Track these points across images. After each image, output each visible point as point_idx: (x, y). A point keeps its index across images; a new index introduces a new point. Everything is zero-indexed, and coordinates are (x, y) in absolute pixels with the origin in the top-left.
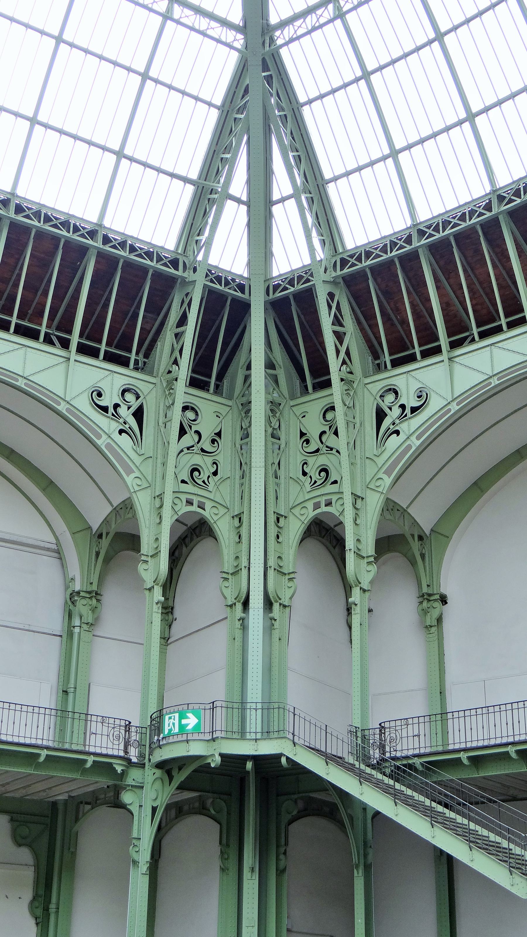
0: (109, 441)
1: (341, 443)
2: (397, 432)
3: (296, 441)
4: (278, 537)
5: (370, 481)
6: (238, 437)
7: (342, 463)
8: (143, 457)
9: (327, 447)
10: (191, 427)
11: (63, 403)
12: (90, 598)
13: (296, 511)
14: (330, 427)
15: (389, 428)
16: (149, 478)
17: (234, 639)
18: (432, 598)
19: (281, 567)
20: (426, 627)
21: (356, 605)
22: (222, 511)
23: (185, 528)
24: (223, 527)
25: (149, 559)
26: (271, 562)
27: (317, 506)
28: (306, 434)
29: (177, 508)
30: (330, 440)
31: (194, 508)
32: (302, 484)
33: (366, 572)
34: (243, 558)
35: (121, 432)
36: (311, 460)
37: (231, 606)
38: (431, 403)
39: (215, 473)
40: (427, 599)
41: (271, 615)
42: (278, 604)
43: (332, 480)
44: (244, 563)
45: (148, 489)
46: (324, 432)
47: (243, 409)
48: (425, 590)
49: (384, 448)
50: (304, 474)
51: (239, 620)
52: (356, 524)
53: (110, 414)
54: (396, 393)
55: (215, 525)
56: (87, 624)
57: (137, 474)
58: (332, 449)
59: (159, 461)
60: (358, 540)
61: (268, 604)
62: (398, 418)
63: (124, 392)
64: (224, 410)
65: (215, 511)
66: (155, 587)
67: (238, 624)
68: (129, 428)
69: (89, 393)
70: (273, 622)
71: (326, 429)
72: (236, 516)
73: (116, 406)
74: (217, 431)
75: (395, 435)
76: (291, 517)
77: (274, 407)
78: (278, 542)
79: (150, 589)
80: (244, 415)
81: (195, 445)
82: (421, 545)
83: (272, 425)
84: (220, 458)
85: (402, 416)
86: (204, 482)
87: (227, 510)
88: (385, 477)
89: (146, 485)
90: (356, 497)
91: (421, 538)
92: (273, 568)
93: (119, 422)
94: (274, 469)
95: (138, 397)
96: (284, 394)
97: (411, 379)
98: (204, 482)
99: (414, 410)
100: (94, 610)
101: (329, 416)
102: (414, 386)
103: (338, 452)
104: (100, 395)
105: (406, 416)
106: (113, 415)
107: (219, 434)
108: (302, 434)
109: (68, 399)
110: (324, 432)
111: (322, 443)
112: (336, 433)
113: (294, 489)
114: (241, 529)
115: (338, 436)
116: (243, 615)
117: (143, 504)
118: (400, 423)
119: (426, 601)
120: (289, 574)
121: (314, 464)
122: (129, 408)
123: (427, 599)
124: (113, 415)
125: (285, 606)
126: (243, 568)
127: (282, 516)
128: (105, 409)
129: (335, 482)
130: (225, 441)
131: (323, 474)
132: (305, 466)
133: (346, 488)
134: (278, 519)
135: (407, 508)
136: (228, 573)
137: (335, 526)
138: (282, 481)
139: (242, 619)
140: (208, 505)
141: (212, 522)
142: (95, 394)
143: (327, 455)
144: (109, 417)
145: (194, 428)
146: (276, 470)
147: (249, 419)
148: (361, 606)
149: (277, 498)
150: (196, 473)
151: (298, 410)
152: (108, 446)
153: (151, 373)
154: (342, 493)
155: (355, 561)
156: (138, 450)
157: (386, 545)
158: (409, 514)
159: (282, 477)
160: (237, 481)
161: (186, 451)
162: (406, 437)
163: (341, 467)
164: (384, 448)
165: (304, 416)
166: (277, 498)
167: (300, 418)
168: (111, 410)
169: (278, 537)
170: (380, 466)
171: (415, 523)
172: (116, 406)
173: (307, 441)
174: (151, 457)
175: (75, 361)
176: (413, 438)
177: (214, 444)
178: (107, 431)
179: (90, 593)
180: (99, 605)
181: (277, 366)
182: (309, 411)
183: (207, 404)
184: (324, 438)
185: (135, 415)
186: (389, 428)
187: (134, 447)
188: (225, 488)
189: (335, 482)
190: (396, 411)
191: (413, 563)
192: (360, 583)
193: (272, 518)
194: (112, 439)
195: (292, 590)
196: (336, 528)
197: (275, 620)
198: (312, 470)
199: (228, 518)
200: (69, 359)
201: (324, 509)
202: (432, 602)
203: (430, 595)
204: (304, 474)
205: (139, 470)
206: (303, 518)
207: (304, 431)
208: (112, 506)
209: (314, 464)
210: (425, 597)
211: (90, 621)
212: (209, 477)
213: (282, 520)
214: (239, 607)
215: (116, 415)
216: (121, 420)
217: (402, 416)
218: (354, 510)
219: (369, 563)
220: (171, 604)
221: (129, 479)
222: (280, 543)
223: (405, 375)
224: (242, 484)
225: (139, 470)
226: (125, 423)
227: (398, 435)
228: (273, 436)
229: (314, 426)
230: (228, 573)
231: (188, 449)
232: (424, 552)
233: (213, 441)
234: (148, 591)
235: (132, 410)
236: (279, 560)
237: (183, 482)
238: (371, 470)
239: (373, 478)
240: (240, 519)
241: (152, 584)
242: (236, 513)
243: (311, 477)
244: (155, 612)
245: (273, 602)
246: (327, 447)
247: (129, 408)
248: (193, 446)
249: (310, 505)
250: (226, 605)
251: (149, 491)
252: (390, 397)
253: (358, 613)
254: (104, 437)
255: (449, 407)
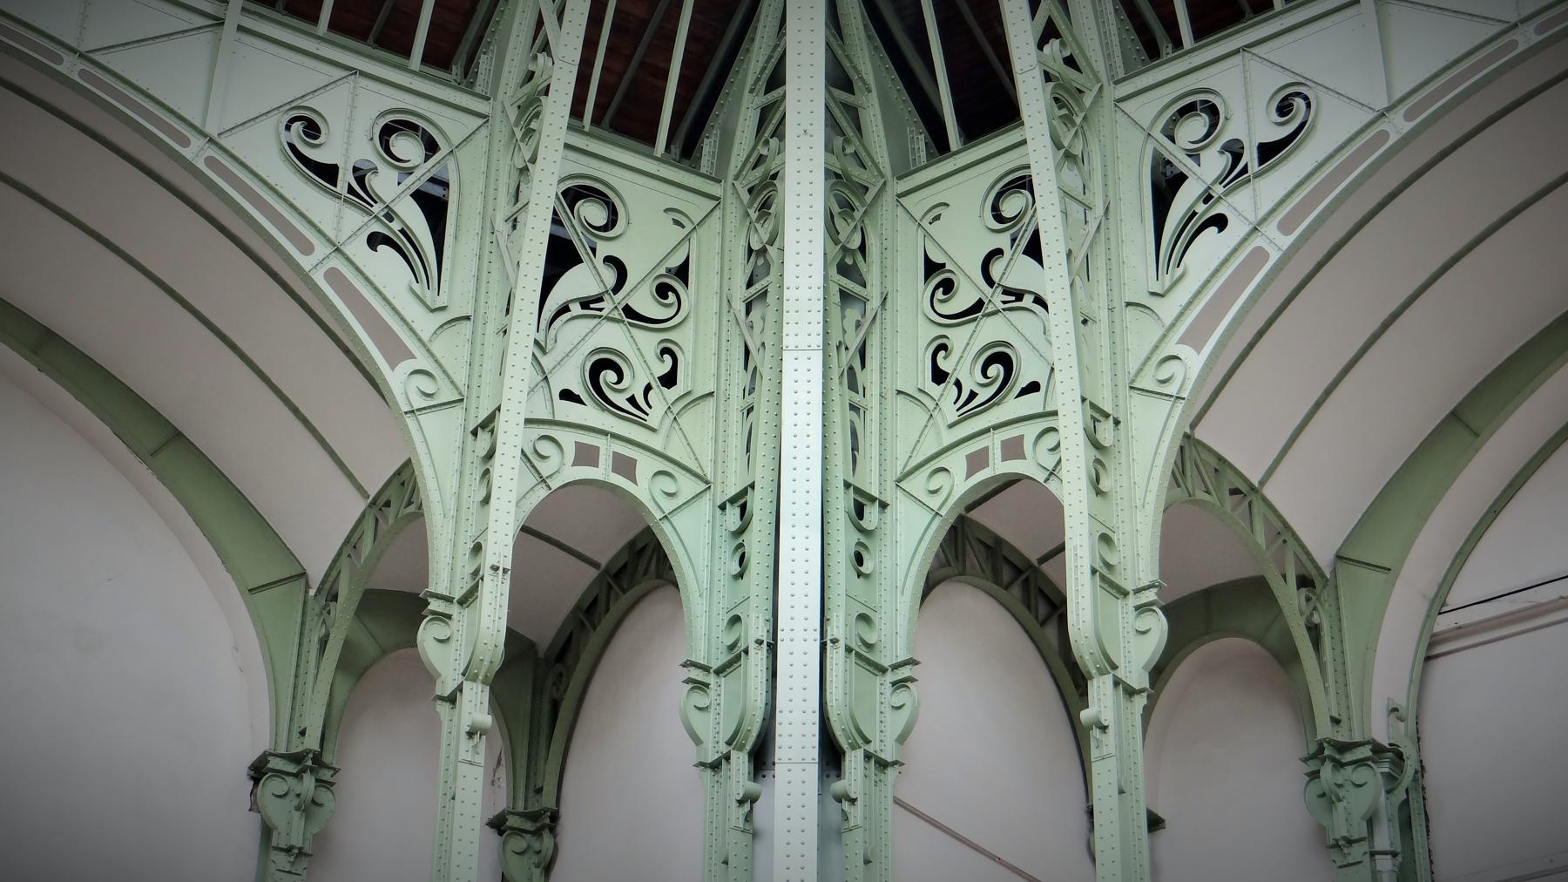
0: (337, 263)
1: (1051, 277)
2: (1220, 222)
3: (912, 290)
4: (859, 559)
5: (1140, 370)
6: (740, 278)
7: (1054, 332)
8: (442, 317)
9: (1007, 291)
10: (594, 250)
11: (197, 142)
12: (298, 776)
13: (917, 484)
14: (1013, 240)
15: (1195, 213)
16: (461, 378)
17: (726, 862)
18: (1348, 757)
19: (869, 646)
20: (1336, 846)
21: (1104, 728)
22: (688, 486)
23: (593, 573)
24: (693, 541)
25: (454, 610)
26: (836, 629)
27: (977, 461)
28: (943, 265)
29: (545, 468)
30: (1017, 271)
31: (602, 472)
32: (931, 405)
33: (1132, 636)
34: (753, 615)
35: (374, 240)
36: (958, 337)
37: (715, 766)
38: (1320, 125)
39: (669, 380)
40: (1333, 760)
41: (838, 786)
42: (860, 753)
43: (1023, 382)
44: (756, 628)
45: (459, 407)
46: (998, 252)
47: (751, 204)
48: (1325, 730)
49: (1179, 271)
50: (939, 376)
51: (741, 802)
52: (1099, 493)
53: (341, 188)
54: (1213, 111)
55: (666, 526)
56: (288, 850)
58: (1019, 295)
59: (492, 328)
60: (1106, 539)
61: (831, 755)
62: (1221, 180)
63: (388, 131)
64: (697, 208)
65: (667, 484)
66: (467, 686)
67: (737, 815)
68: (402, 231)
69: (279, 122)
70: (846, 805)
71: (1003, 241)
72: (732, 501)
74: (675, 262)
75: (1213, 230)
76: (901, 507)
77: (847, 195)
78: (860, 575)
79: (452, 699)
80: (754, 215)
81: (606, 297)
82: (1308, 600)
83: (842, 237)
84: (683, 338)
85: (1235, 174)
86: (632, 400)
87: (704, 486)
88: (1185, 351)
89: (448, 395)
90: (1098, 414)
91: (1304, 582)
92: (842, 644)
93: (369, 213)
94: (849, 369)
95: (431, 147)
96: (879, 160)
97: (1255, 67)
98: (632, 400)
99: (1268, 151)
100: (308, 808)
101: (1010, 207)
102: (1269, 83)
103: (1039, 301)
104: (312, 130)
105: (1245, 170)
107: (682, 272)
108: (931, 268)
109: (212, 130)
110: (998, 252)
111: (990, 282)
112: (1034, 250)
113: (908, 420)
114: (744, 537)
115: (1040, 262)
116: (753, 787)
117: (438, 449)
118: (1227, 194)
119: (1328, 766)
120: (895, 667)
121: (968, 343)
123: (1333, 760)
124: (351, 190)
125: (883, 765)
126: (752, 647)
127: (872, 499)
128: (328, 173)
129: (1033, 387)
130: (699, 295)
131: (996, 370)
132: (942, 353)
133: (1066, 399)
134: (860, 511)
135: (1262, 483)
136: (706, 669)
137: (1043, 560)
138: (872, 402)
139: (749, 799)
140: (646, 466)
141: (658, 515)
143: (1008, 314)
144: (338, 196)
145: (604, 249)
146: (851, 369)
147: (769, 225)
148: (1119, 734)
149: (855, 448)
150: (609, 376)
151: (918, 204)
152: (333, 276)
153: (467, 80)
154: (1055, 413)
155: (1095, 607)
156: (429, 296)
157: (1202, 613)
158: (1265, 499)
159: (874, 390)
160: (737, 403)
161: (576, 309)
162: (1247, 229)
163: (1048, 344)
164: (1179, 271)
165: (937, 218)
166: (855, 448)
167: (925, 223)
168: (346, 178)
169: (859, 559)
170: (1168, 321)
171: (1283, 532)
173: (948, 286)
174: (468, 318)
175: (241, 29)
176: (1271, 229)
177: (666, 297)
178: (331, 234)
179: (297, 758)
180: (324, 796)
181: (857, 85)
182: (953, 209)
183: (645, 188)
184: (996, 270)
185: (420, 197)
186: (1195, 213)
187: (416, 286)
188: (699, 422)
189: (1033, 387)
190: (1214, 162)
191: (1287, 657)
192: (1114, 667)
193: (842, 503)
194: (348, 259)
195: (904, 715)
196: (1045, 567)
197: (853, 801)
198: (963, 365)
199: (706, 506)
200: (219, 22)
201: (999, 466)
202: (1350, 768)
203: (1343, 748)
204: (939, 376)
205: (428, 350)
206: (935, 502)
207: (937, 258)
208: (365, 495)
209: (968, 343)
210: (1326, 752)
211: (296, 841)
212: (648, 388)
213: (871, 512)
214: (741, 762)
216: (377, 208)
217: (1235, 174)
218: (1094, 453)
219: (1142, 609)
220: (548, 801)
221: (396, 378)
222: (867, 576)
223: (1236, 59)
224: (750, 410)
225: (428, 350)
226: (390, 216)
227: (1221, 229)
228: (845, 270)
229: (965, 238)
230: (706, 669)
231: (585, 304)
232: (1316, 619)
233: (663, 291)
234: (447, 706)
236: (863, 627)
237: (567, 395)
238: (1140, 335)
239: (1148, 358)
240: (743, 508)
241: (461, 678)
242: (732, 492)
243: (958, 384)
244: (464, 761)
245: (845, 746)
246: (1007, 291)
248: (600, 299)
249: (957, 462)
250: (702, 764)
251: (457, 412)
252: (1195, 127)
253: (1110, 756)
254: (321, 249)
255: (1382, 126)
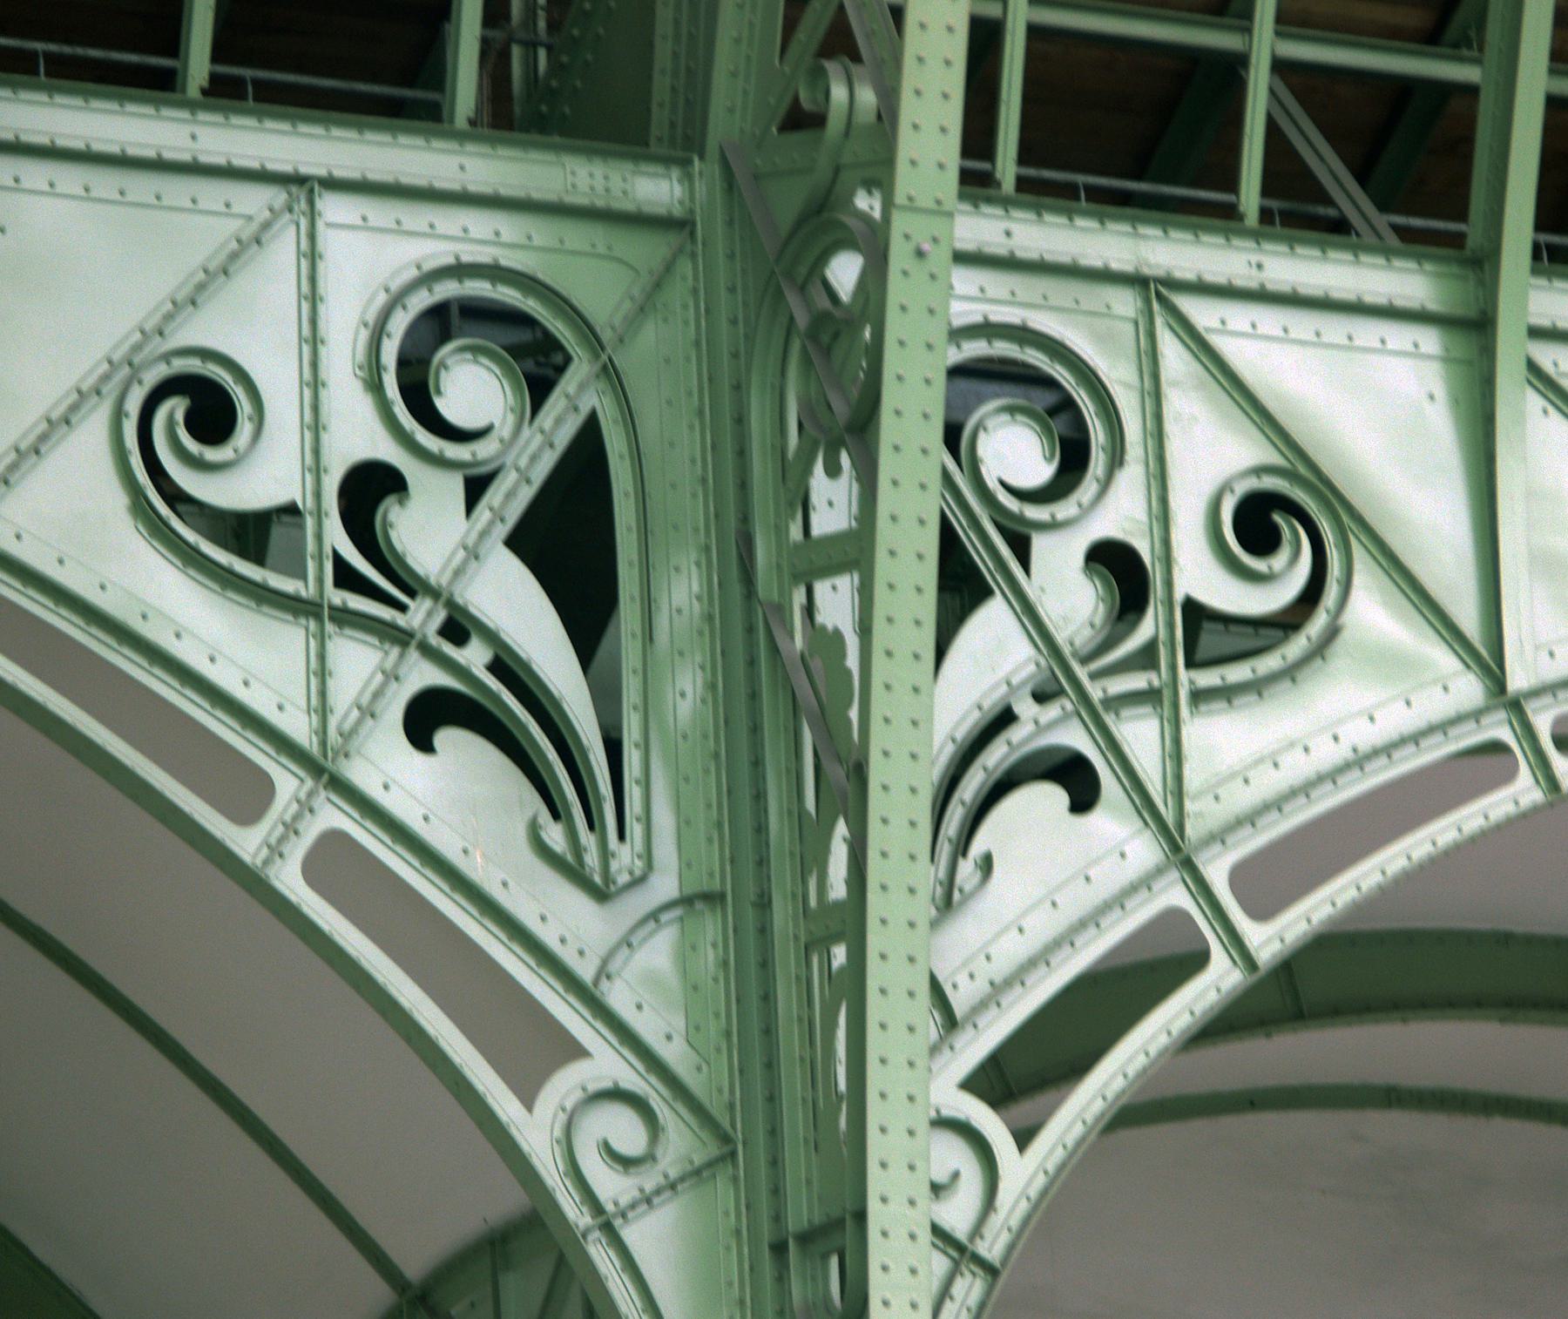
0: (333, 816)
35: (425, 719)
57: (607, 1064)
69: (118, 414)
73: (369, 489)
93: (400, 637)
104: (211, 408)
106: (346, 577)
122: (476, 488)
124: (346, 577)
142: (175, 408)
172: (369, 489)
185: (530, 541)
215: (378, 577)
216: (422, 616)
226: (458, 628)
235: (511, 498)
247: (476, 488)
